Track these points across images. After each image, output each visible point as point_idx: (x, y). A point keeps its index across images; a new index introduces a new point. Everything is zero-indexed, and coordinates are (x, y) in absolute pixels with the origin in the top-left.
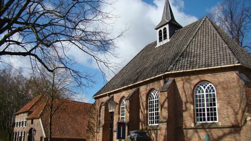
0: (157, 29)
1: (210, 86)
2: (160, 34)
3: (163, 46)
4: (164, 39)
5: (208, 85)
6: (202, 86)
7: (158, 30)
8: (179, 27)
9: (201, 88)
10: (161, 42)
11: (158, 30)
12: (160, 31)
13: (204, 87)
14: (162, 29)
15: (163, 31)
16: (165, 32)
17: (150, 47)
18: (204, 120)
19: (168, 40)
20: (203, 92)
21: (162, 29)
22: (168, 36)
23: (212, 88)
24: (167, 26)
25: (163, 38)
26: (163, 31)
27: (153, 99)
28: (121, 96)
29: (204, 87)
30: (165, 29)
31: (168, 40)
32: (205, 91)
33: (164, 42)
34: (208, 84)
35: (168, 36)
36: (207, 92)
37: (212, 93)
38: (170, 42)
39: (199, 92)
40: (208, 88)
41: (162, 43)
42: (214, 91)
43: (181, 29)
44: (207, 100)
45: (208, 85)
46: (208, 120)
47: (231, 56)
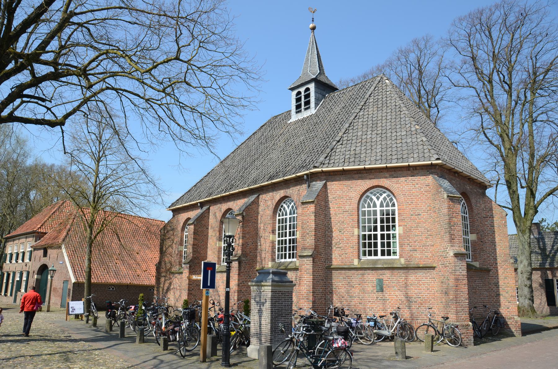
0: (292, 89)
2: (298, 100)
3: (303, 120)
4: (305, 109)
6: (375, 195)
7: (295, 92)
8: (333, 89)
9: (371, 200)
10: (299, 114)
11: (295, 92)
12: (299, 93)
13: (378, 198)
14: (302, 90)
15: (303, 94)
16: (307, 96)
18: (376, 254)
19: (312, 111)
20: (375, 206)
21: (302, 90)
25: (303, 107)
26: (303, 94)
27: (286, 215)
29: (378, 198)
30: (308, 89)
31: (312, 111)
32: (378, 203)
33: (305, 114)
35: (312, 104)
36: (382, 205)
38: (316, 115)
39: (369, 206)
40: (385, 199)
41: (300, 116)
42: (393, 205)
43: (336, 93)
46: (383, 254)
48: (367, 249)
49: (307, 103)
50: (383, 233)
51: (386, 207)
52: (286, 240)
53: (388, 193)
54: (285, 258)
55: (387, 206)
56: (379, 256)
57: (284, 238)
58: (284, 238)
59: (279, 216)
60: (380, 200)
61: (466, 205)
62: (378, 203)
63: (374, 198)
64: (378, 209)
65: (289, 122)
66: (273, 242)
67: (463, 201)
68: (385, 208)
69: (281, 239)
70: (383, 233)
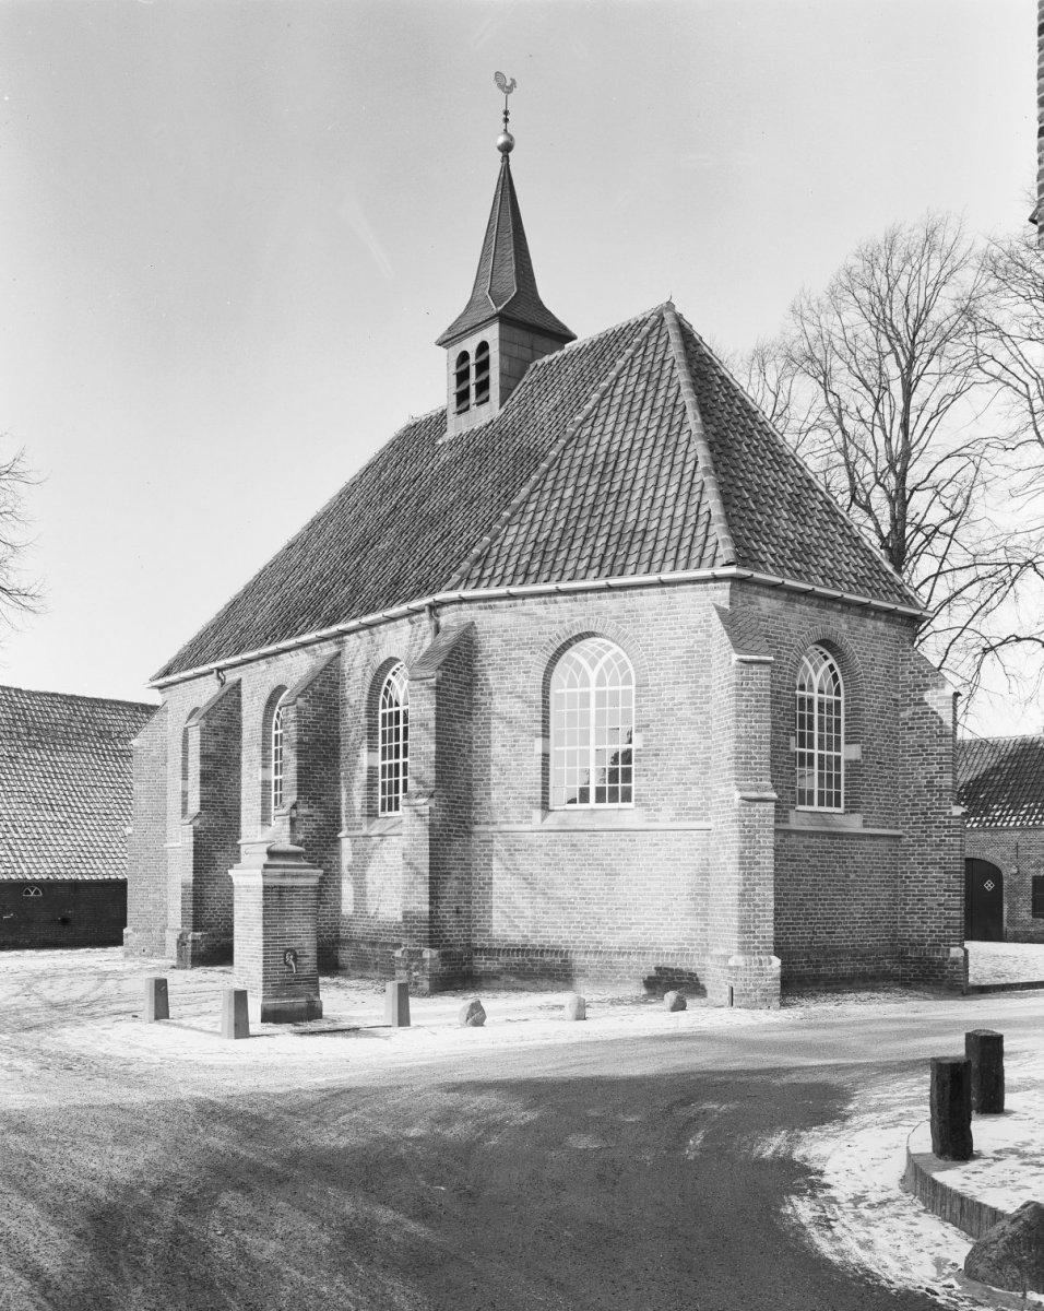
1: (617, 657)
2: (462, 376)
4: (478, 404)
5: (608, 655)
12: (464, 356)
13: (593, 663)
14: (470, 345)
15: (472, 360)
16: (483, 366)
17: (420, 436)
20: (586, 683)
21: (470, 345)
23: (623, 667)
24: (492, 334)
25: (473, 398)
26: (472, 360)
29: (593, 663)
30: (483, 347)
32: (593, 676)
34: (608, 648)
35: (494, 391)
36: (600, 681)
37: (621, 688)
40: (608, 665)
44: (600, 716)
45: (608, 655)
47: (712, 530)
49: (483, 386)
51: (611, 685)
52: (397, 765)
53: (616, 649)
55: (614, 682)
56: (592, 803)
57: (394, 761)
59: (384, 707)
60: (597, 669)
62: (593, 676)
65: (440, 442)
66: (372, 770)
67: (831, 660)
68: (608, 688)
69: (387, 762)
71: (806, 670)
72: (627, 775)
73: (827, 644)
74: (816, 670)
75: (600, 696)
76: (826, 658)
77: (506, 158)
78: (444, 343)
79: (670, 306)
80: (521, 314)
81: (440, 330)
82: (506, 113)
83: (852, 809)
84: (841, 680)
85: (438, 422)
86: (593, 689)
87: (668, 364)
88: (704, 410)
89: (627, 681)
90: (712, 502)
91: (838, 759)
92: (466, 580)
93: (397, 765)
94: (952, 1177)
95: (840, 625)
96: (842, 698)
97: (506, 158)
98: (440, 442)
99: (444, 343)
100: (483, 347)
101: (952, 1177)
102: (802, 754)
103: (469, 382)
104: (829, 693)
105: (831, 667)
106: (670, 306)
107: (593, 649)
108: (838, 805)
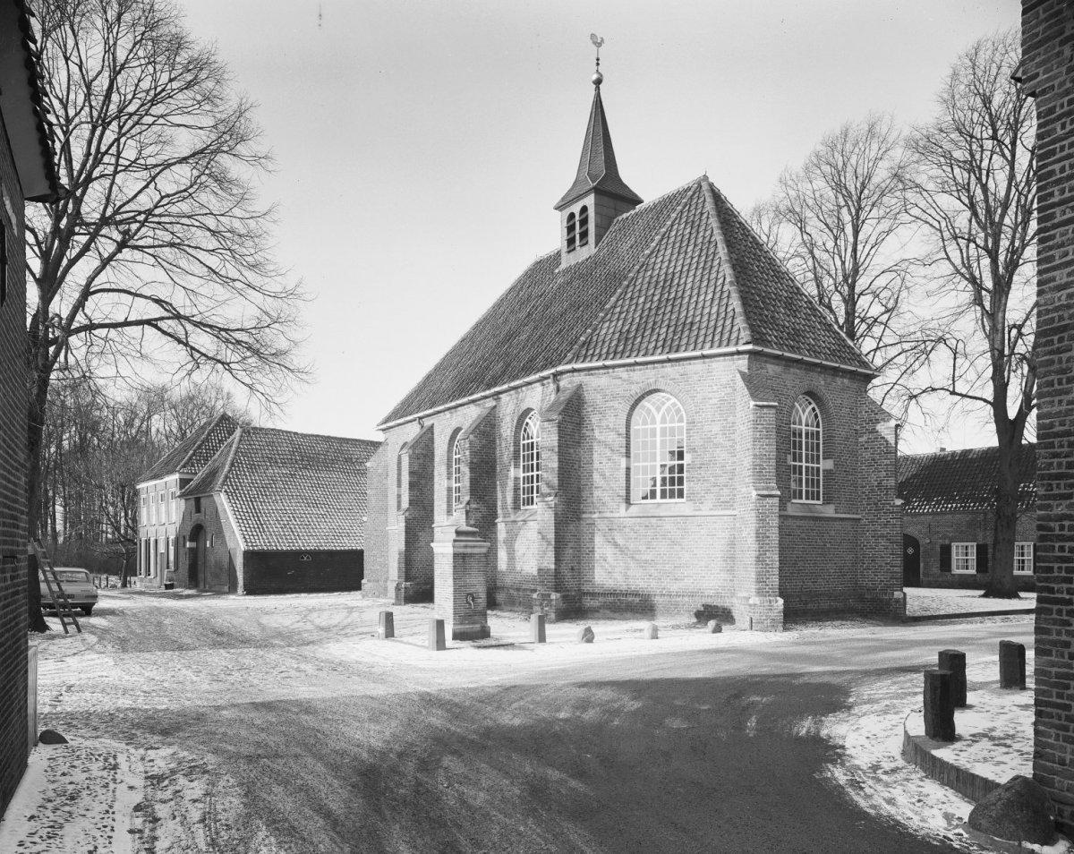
2: (571, 229)
4: (581, 246)
5: (668, 404)
7: (567, 212)
11: (567, 212)
12: (572, 216)
13: (658, 409)
14: (576, 208)
15: (577, 218)
16: (584, 222)
17: (545, 267)
20: (653, 422)
21: (576, 208)
22: (592, 237)
23: (678, 411)
24: (590, 201)
25: (578, 243)
26: (577, 218)
28: (454, 425)
29: (658, 409)
30: (584, 209)
32: (658, 418)
34: (668, 399)
35: (592, 237)
36: (663, 420)
37: (676, 425)
39: (645, 423)
40: (668, 410)
44: (663, 442)
45: (668, 404)
47: (736, 321)
48: (668, 487)
49: (584, 235)
50: (680, 462)
52: (532, 476)
53: (673, 400)
54: (801, 498)
55: (672, 421)
56: (658, 500)
57: (530, 474)
58: (530, 474)
61: (817, 411)
62: (658, 418)
63: (653, 410)
64: (658, 426)
65: (557, 271)
66: (516, 479)
67: (813, 405)
68: (668, 425)
69: (526, 474)
70: (680, 462)
71: (797, 411)
72: (681, 481)
73: (811, 394)
74: (804, 411)
75: (663, 431)
76: (810, 403)
77: (598, 88)
78: (559, 208)
79: (705, 178)
80: (610, 187)
81: (557, 199)
82: (598, 59)
83: (827, 501)
84: (820, 418)
85: (557, 257)
86: (658, 426)
87: (705, 215)
88: (729, 244)
89: (681, 420)
90: (736, 303)
91: (818, 469)
92: (576, 357)
93: (532, 476)
94: (945, 754)
95: (819, 382)
96: (821, 430)
97: (598, 88)
98: (557, 271)
99: (559, 208)
100: (584, 209)
101: (945, 754)
102: (795, 466)
103: (575, 232)
104: (812, 426)
105: (814, 409)
106: (705, 178)
107: (658, 400)
108: (818, 499)
